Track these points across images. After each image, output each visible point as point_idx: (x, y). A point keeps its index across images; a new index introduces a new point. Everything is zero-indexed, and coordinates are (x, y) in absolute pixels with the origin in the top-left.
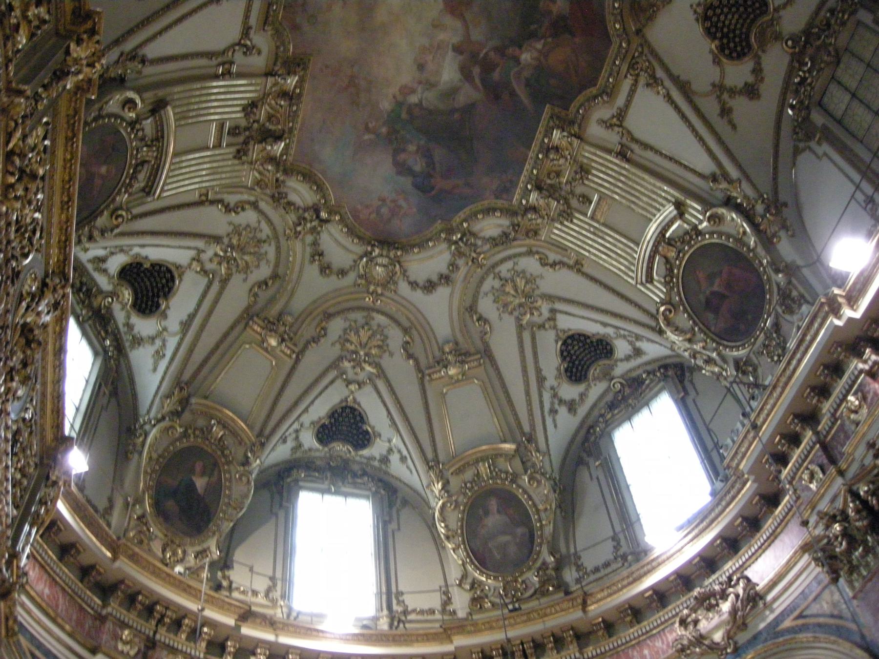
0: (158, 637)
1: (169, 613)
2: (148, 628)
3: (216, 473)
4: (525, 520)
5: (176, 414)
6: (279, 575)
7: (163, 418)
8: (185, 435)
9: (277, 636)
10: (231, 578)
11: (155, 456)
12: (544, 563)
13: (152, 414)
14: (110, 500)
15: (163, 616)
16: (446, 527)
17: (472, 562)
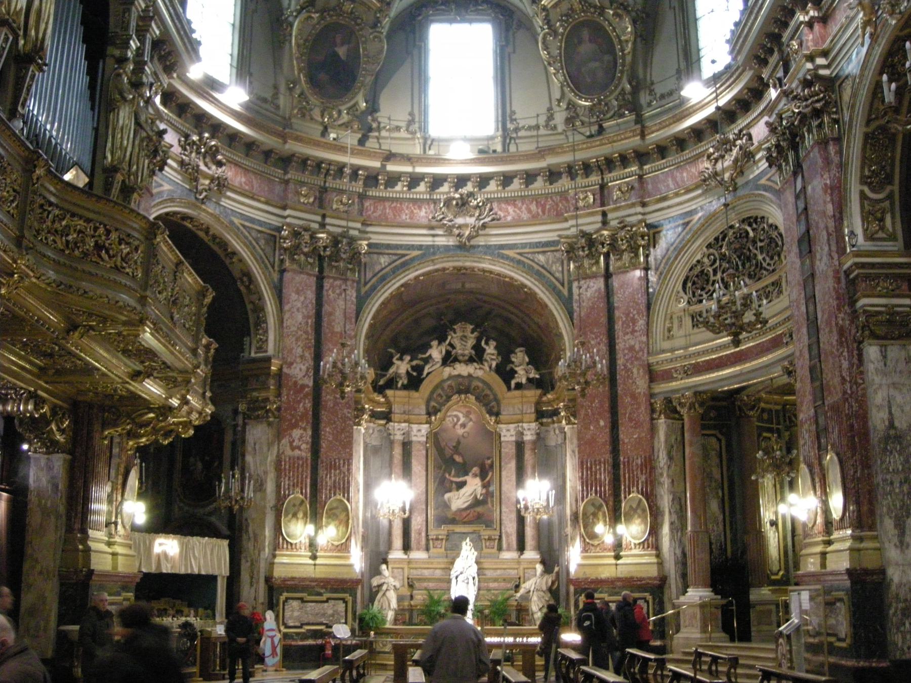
0: (327, 185)
1: (332, 167)
2: (319, 181)
4: (611, 50)
6: (416, 112)
7: (302, 8)
8: (322, 18)
9: (414, 167)
10: (379, 119)
11: (302, 42)
12: (623, 89)
13: (293, 7)
14: (276, 87)
15: (328, 170)
16: (549, 53)
17: (569, 86)
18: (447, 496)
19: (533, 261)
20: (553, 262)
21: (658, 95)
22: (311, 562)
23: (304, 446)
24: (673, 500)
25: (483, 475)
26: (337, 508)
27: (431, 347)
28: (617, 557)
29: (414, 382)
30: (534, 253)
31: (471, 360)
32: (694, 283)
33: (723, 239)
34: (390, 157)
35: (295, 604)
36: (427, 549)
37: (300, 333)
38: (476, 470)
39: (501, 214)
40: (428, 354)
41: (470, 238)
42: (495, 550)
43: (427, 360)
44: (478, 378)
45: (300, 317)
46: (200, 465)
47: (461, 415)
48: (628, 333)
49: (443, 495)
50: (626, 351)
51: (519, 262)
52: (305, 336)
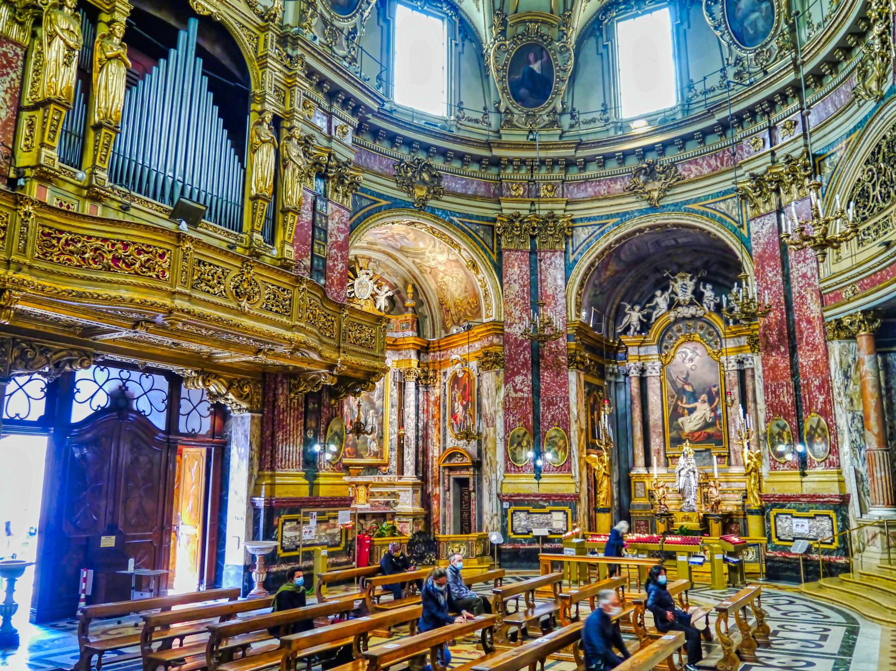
3: (544, 53)
5: (503, 33)
13: (489, 42)
16: (714, 19)
17: (735, 43)
18: (680, 420)
19: (715, 210)
20: (733, 207)
21: (815, 26)
22: (536, 481)
23: (526, 389)
24: (853, 418)
25: (711, 400)
26: (555, 436)
27: (654, 296)
28: (803, 475)
29: (645, 326)
30: (716, 202)
31: (691, 303)
32: (857, 203)
33: (879, 153)
34: (579, 145)
35: (522, 515)
36: (667, 465)
37: (517, 299)
38: (704, 397)
39: (686, 174)
40: (654, 303)
41: (659, 199)
42: (725, 465)
43: (654, 308)
44: (700, 318)
45: (516, 287)
46: (461, 408)
47: (688, 351)
48: (800, 262)
49: (677, 420)
50: (800, 279)
51: (703, 213)
52: (522, 301)
